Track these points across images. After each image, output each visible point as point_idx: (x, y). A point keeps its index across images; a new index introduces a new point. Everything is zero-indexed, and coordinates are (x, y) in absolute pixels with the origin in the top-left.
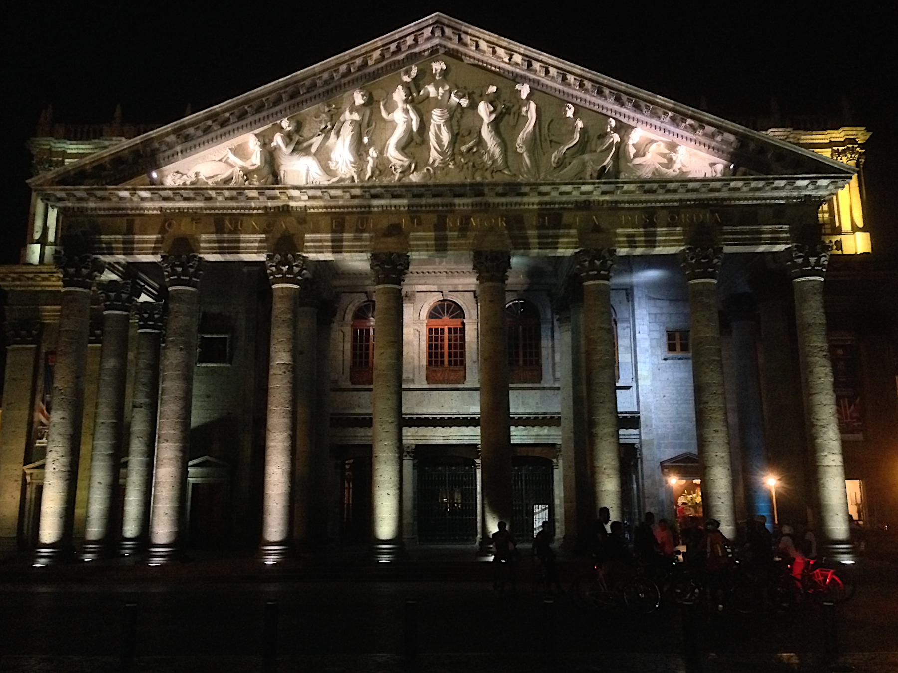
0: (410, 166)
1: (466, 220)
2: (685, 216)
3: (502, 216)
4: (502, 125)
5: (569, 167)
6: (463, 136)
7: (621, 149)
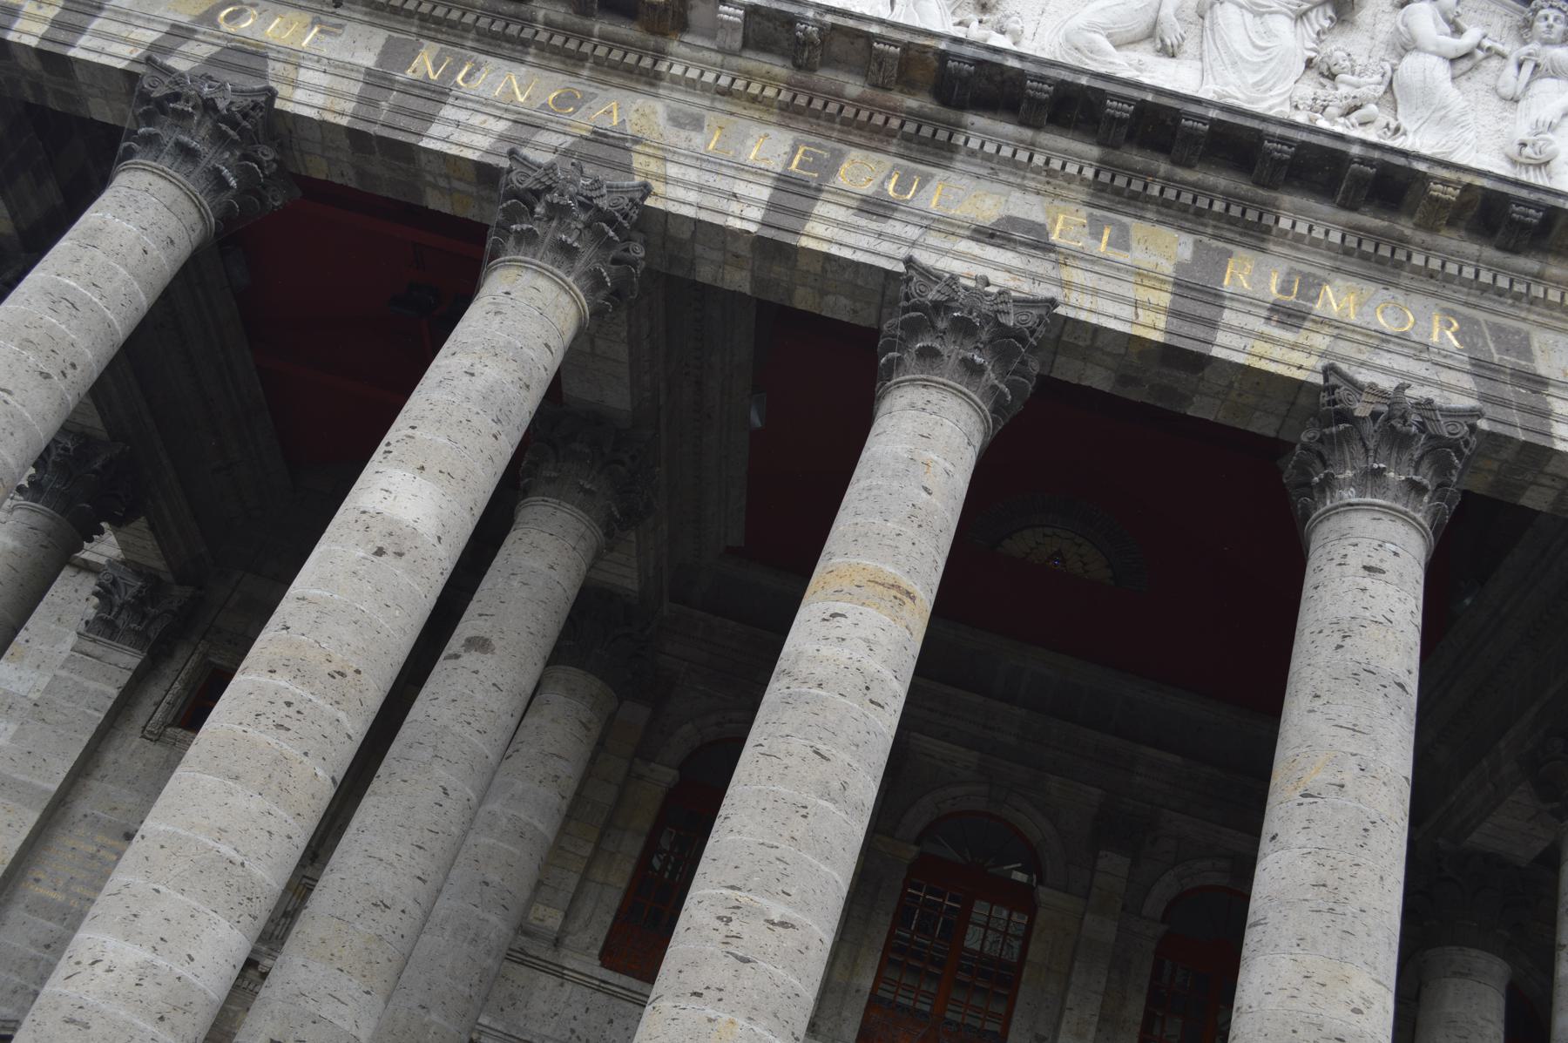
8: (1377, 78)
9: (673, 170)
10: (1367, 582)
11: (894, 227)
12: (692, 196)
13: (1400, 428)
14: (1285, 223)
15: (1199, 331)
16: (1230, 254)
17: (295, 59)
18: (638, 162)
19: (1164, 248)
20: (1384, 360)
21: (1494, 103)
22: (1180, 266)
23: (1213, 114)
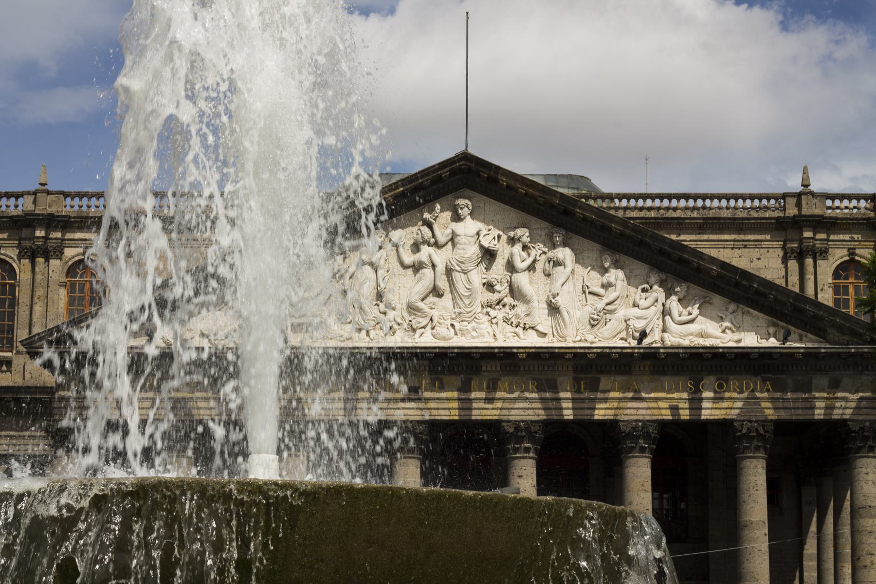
0: (431, 320)
2: (734, 384)
3: (533, 379)
5: (608, 324)
7: (667, 306)
8: (506, 284)
10: (520, 481)
13: (523, 430)
14: (484, 368)
15: (467, 412)
16: (471, 379)
20: (518, 405)
23: (456, 351)
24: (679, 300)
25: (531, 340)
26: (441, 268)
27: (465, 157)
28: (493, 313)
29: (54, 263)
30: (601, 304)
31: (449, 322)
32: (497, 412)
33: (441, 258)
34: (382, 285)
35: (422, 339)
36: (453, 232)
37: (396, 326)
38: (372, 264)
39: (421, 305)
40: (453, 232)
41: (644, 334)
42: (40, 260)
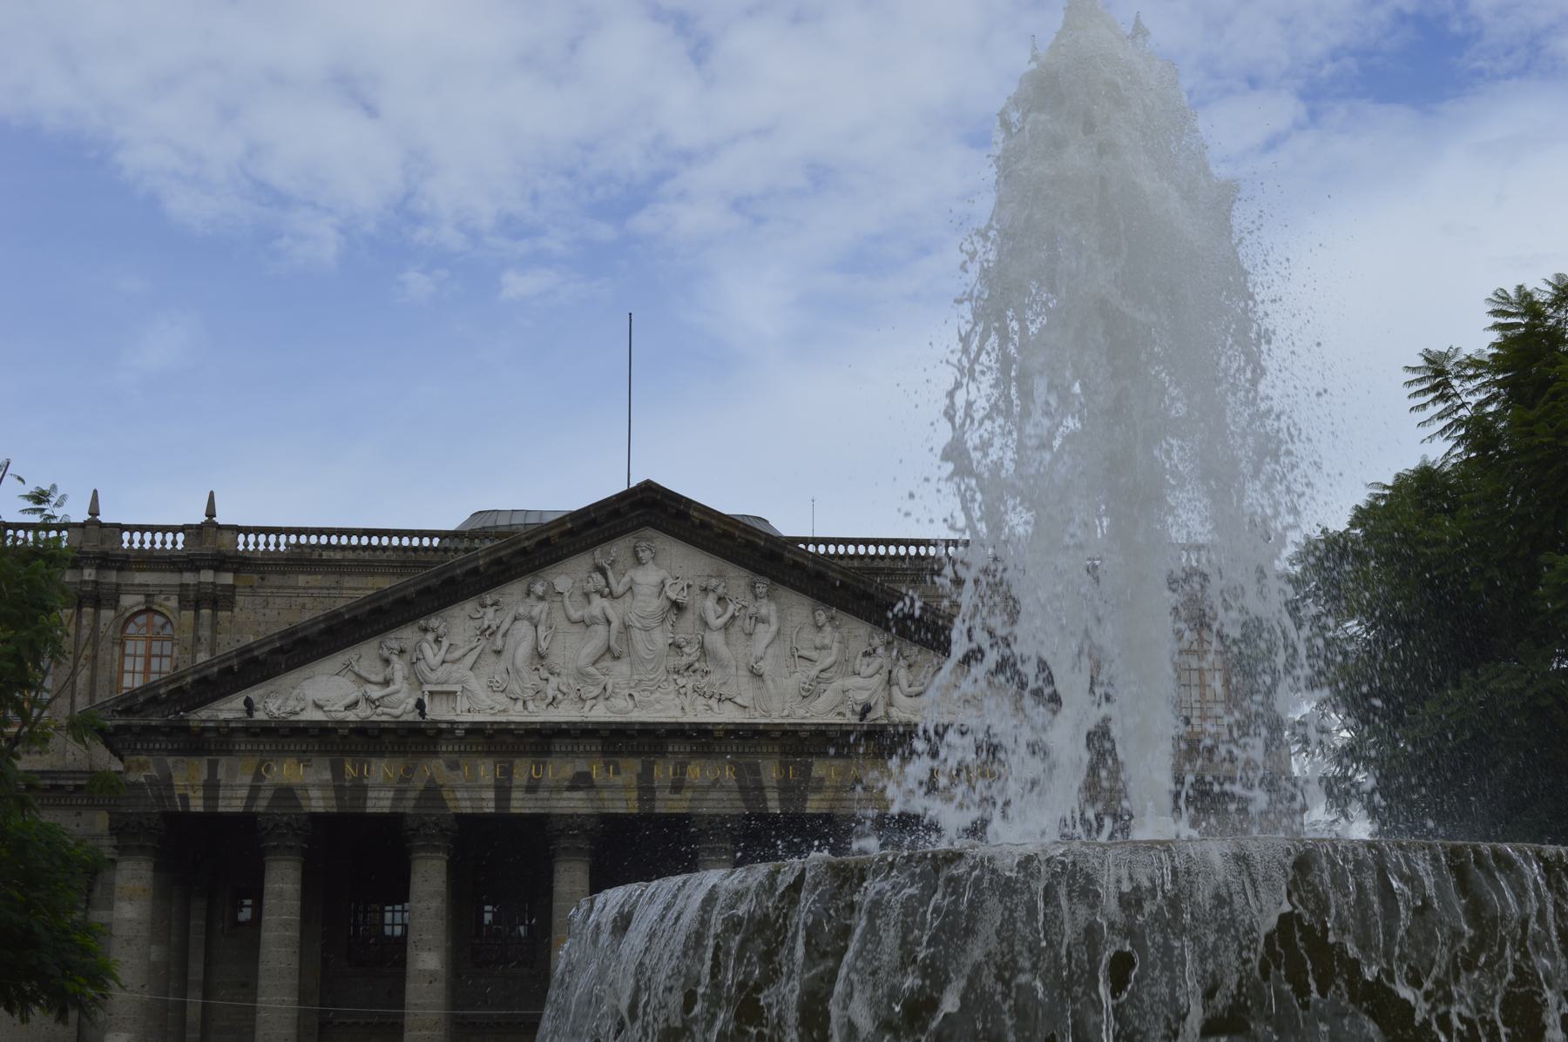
1: (682, 767)
3: (731, 762)
4: (732, 630)
6: (679, 647)
9: (459, 795)
11: (542, 794)
12: (468, 803)
16: (654, 763)
17: (304, 788)
18: (445, 794)
19: (631, 768)
21: (743, 636)
22: (639, 776)
24: (910, 666)
25: (727, 715)
26: (615, 624)
27: (649, 488)
28: (681, 681)
29: (107, 614)
30: (814, 672)
31: (627, 692)
32: (686, 804)
33: (614, 610)
34: (544, 645)
35: (593, 713)
36: (632, 580)
37: (560, 696)
38: (530, 619)
39: (592, 670)
40: (632, 580)
41: (867, 709)
42: (88, 610)
